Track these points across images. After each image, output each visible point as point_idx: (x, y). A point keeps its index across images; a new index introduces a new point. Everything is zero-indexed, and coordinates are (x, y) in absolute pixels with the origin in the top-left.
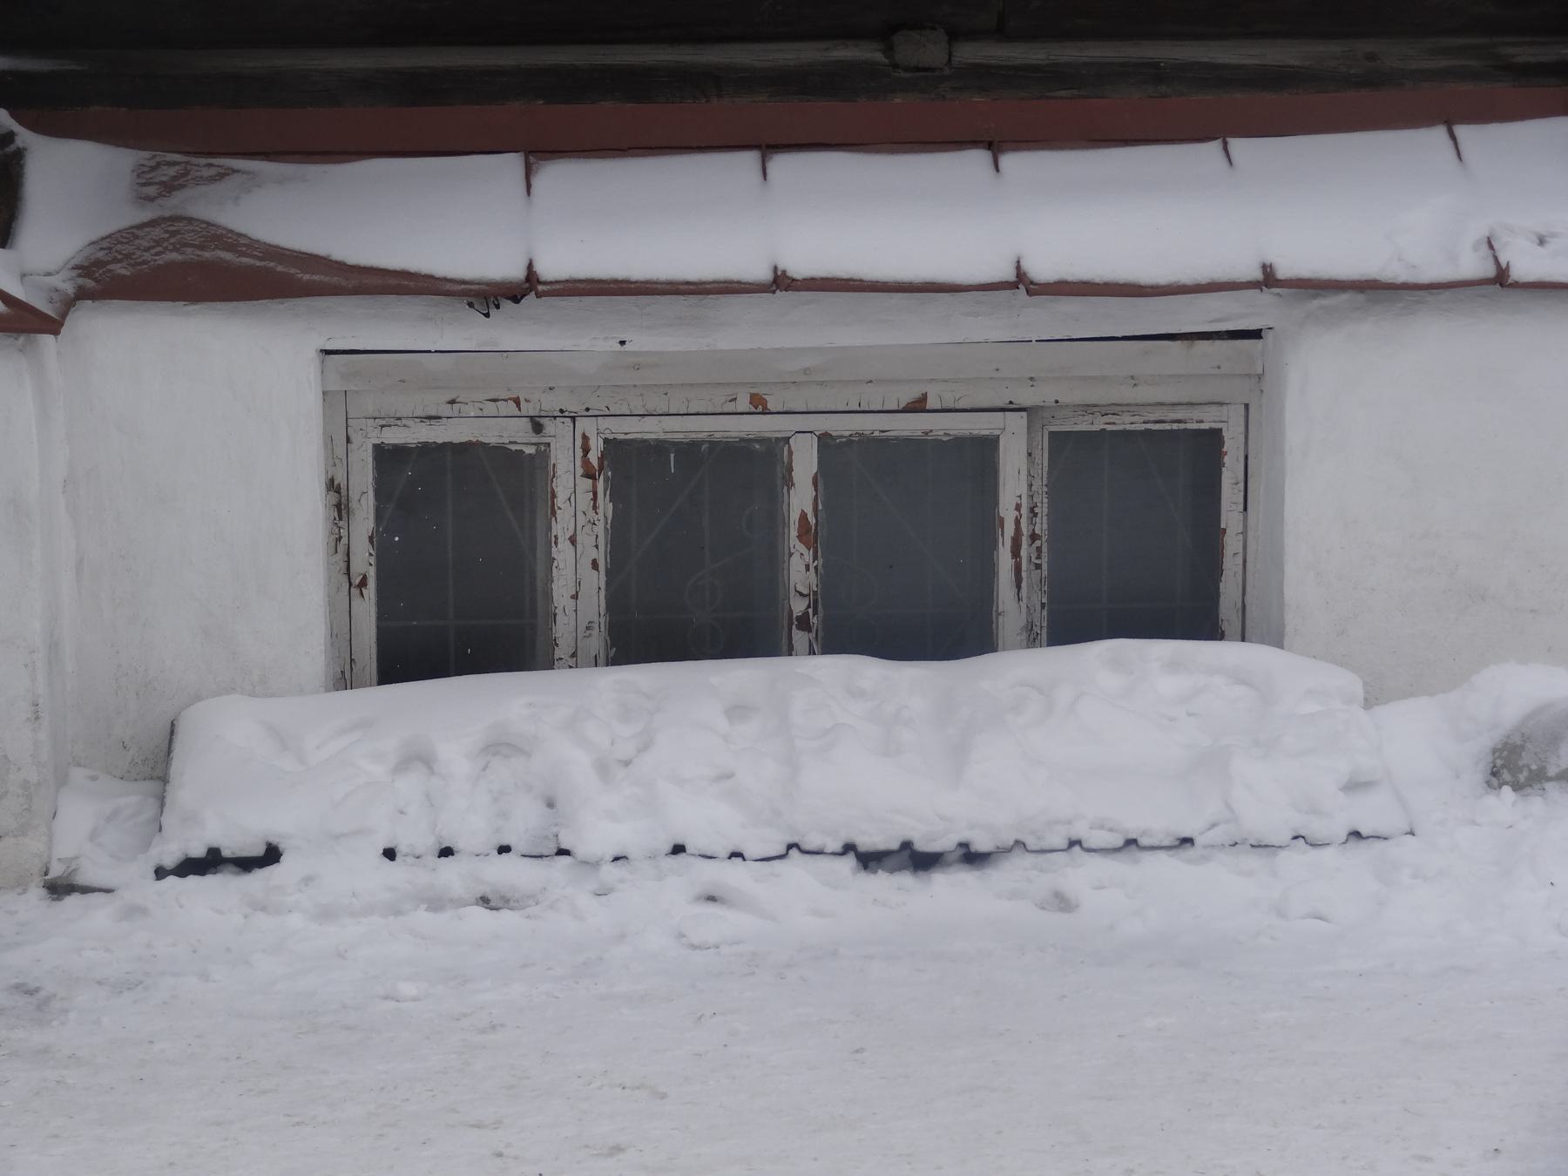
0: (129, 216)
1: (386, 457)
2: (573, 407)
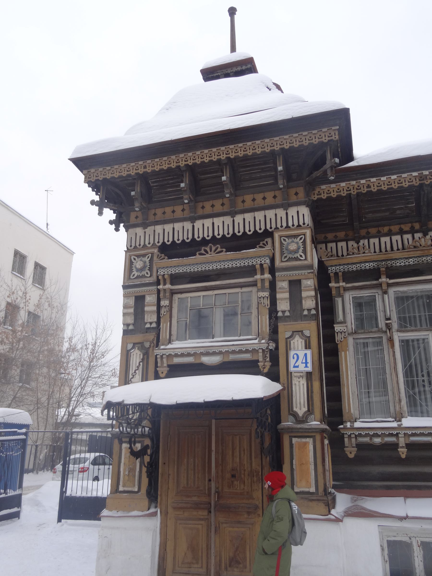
0: (351, 505)
1: (389, 542)
2: (416, 536)
